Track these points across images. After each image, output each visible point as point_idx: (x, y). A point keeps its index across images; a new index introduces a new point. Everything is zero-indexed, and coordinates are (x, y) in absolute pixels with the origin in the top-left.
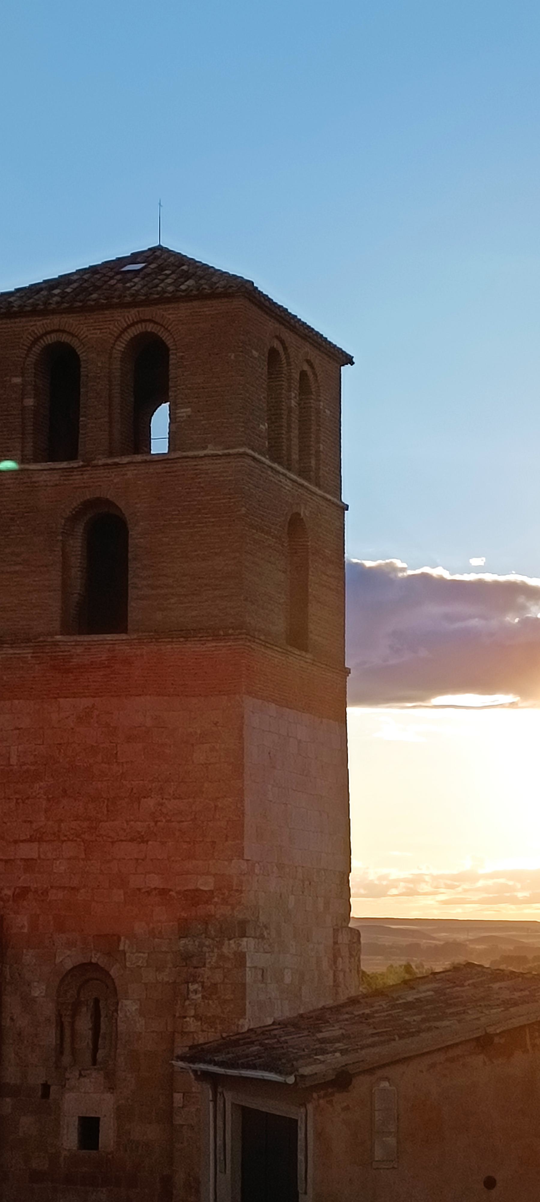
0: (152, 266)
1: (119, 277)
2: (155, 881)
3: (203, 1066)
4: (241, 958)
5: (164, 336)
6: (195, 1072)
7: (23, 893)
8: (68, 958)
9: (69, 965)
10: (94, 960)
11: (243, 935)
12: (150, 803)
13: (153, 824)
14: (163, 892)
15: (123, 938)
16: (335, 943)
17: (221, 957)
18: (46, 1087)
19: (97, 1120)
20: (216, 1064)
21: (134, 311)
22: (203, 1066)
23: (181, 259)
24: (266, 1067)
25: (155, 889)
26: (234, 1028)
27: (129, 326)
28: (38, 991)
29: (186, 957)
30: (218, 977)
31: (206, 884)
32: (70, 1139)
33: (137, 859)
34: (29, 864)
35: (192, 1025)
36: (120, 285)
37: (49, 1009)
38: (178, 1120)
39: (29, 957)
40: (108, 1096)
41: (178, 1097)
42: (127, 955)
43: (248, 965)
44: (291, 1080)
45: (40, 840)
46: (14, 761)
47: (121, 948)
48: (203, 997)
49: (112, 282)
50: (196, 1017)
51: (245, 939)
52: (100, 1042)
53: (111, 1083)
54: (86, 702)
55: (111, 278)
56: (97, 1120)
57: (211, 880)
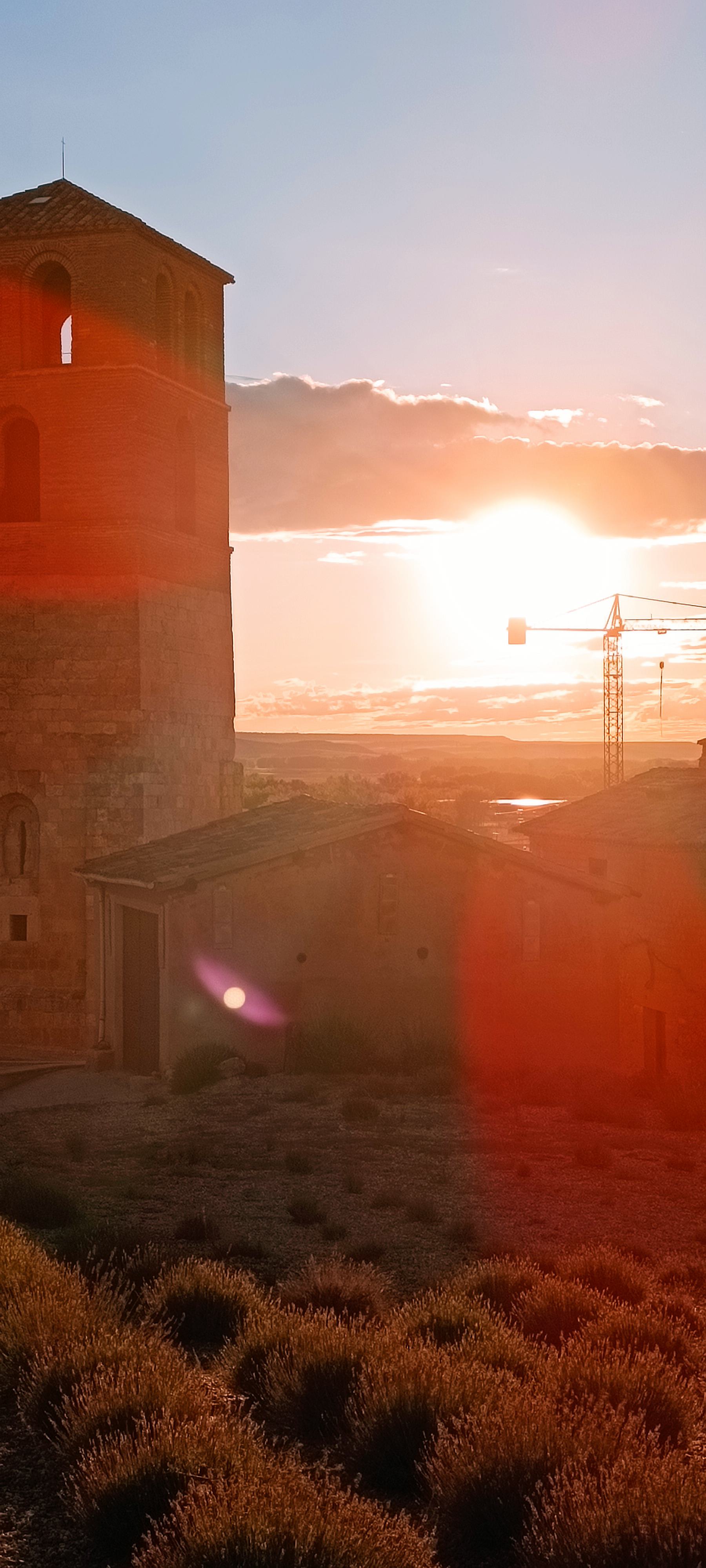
0: (56, 200)
1: (27, 209)
3: (92, 876)
4: (139, 788)
6: (88, 880)
10: (19, 791)
11: (140, 770)
13: (65, 681)
15: (42, 773)
16: (221, 774)
20: (105, 874)
21: (39, 242)
22: (92, 876)
23: (81, 194)
24: (135, 877)
25: (68, 733)
26: (134, 844)
27: (36, 256)
33: (53, 709)
36: (28, 218)
42: (47, 786)
43: (145, 794)
44: (151, 886)
47: (41, 781)
48: (109, 820)
49: (22, 215)
51: (142, 774)
52: (26, 856)
55: (21, 211)
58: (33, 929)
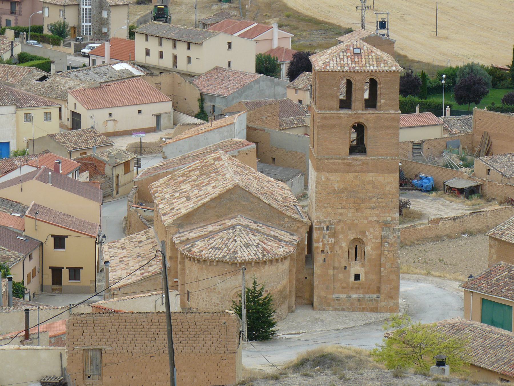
2: (376, 218)
5: (377, 80)
7: (340, 221)
8: (352, 237)
9: (352, 238)
12: (374, 200)
14: (378, 221)
17: (394, 236)
18: (346, 267)
19: (359, 274)
28: (344, 244)
29: (385, 237)
30: (393, 241)
31: (389, 219)
32: (353, 278)
34: (341, 214)
35: (386, 252)
37: (347, 249)
38: (382, 274)
39: (341, 236)
40: (362, 269)
41: (382, 269)
45: (344, 208)
46: (336, 188)
50: (388, 251)
53: (363, 266)
54: (356, 174)
56: (359, 274)
57: (390, 218)
58: (362, 277)
